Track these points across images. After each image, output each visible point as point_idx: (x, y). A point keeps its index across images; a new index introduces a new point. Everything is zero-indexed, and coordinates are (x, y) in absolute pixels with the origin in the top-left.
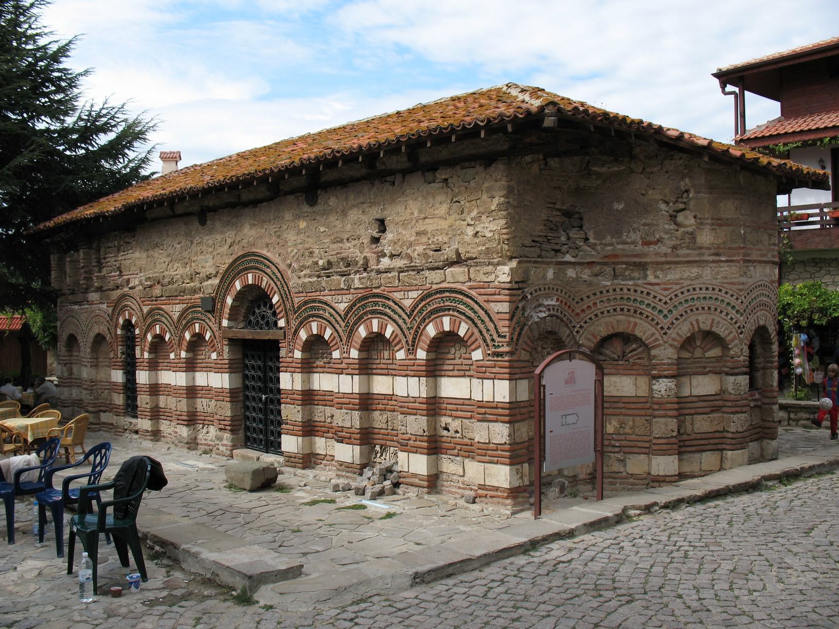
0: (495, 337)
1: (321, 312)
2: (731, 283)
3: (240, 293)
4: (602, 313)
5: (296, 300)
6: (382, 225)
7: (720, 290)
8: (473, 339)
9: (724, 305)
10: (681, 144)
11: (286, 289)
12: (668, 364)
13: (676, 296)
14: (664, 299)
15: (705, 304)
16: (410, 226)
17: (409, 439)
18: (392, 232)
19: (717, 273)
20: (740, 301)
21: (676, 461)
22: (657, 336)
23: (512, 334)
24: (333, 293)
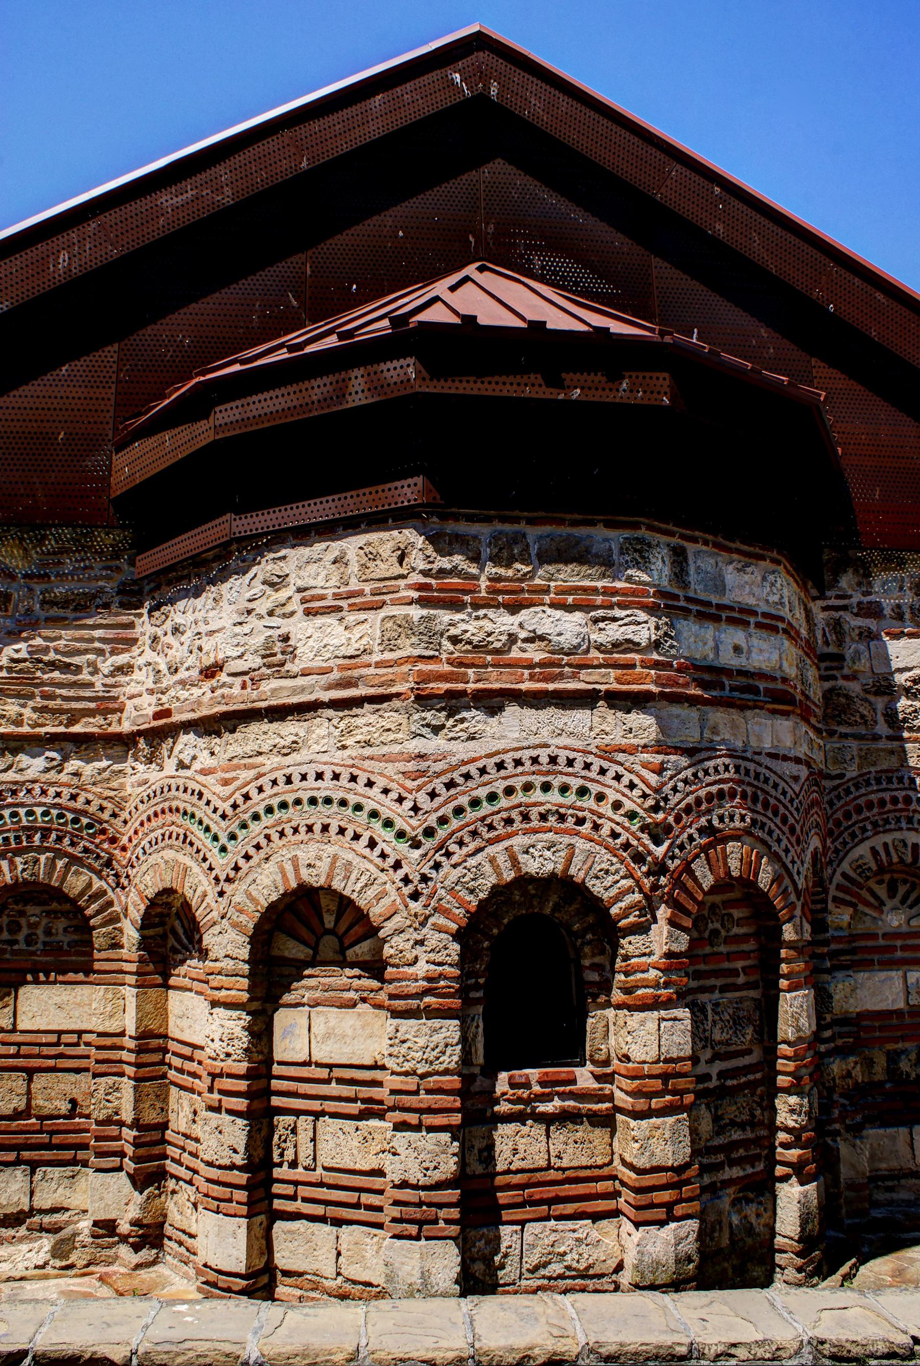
2: (384, 758)
7: (353, 779)
13: (247, 797)
15: (317, 816)
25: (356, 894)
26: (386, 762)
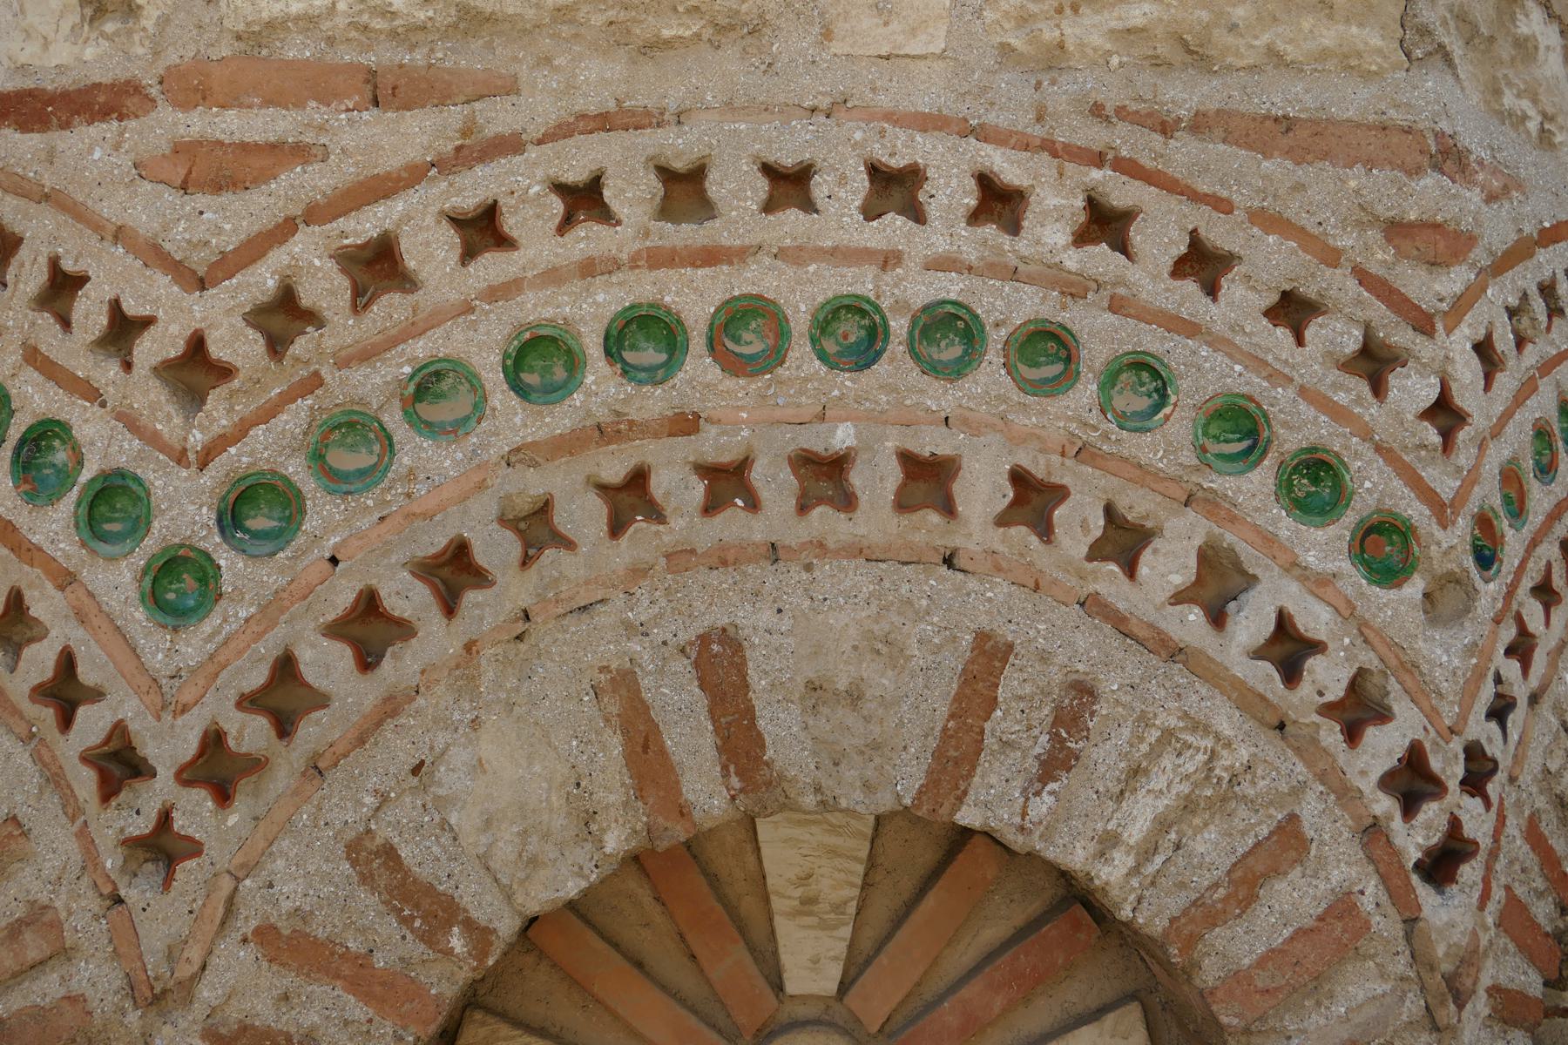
2: (1280, 134)
7: (1104, 224)
9: (1169, 444)
13: (378, 266)
14: (175, 317)
15: (874, 414)
20: (1413, 390)
25: (1122, 861)
26: (1299, 155)
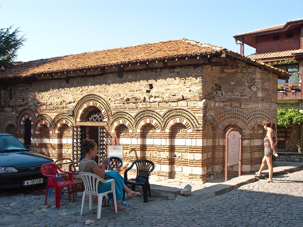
0: (197, 125)
1: (124, 116)
2: (267, 109)
3: (85, 109)
4: (227, 118)
5: (113, 112)
6: (151, 86)
7: (263, 112)
8: (189, 125)
10: (255, 64)
11: (108, 107)
12: (248, 135)
13: (251, 113)
16: (163, 87)
17: (161, 160)
18: (156, 89)
19: (263, 106)
21: (250, 167)
22: (244, 125)
23: (203, 124)
24: (130, 109)
